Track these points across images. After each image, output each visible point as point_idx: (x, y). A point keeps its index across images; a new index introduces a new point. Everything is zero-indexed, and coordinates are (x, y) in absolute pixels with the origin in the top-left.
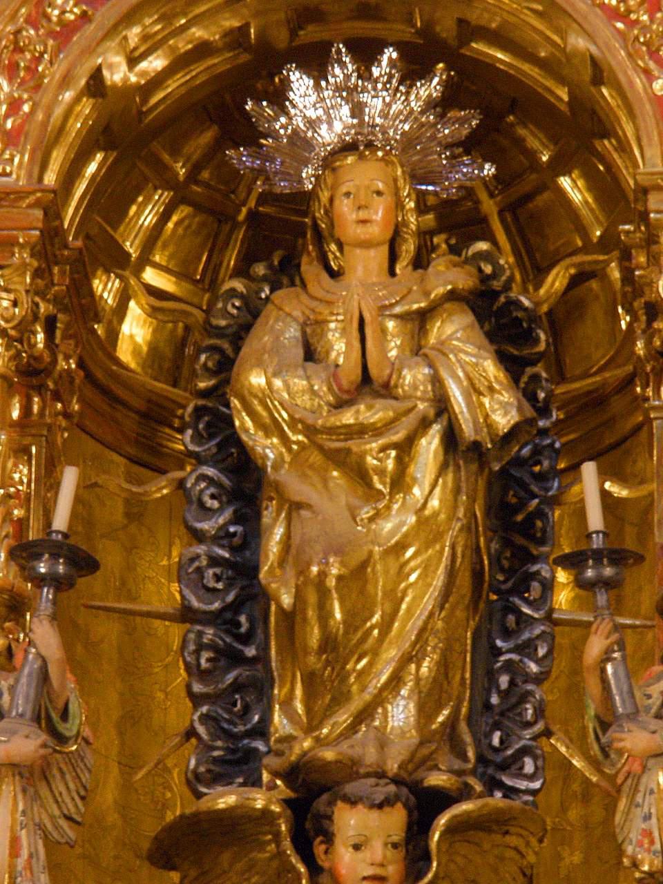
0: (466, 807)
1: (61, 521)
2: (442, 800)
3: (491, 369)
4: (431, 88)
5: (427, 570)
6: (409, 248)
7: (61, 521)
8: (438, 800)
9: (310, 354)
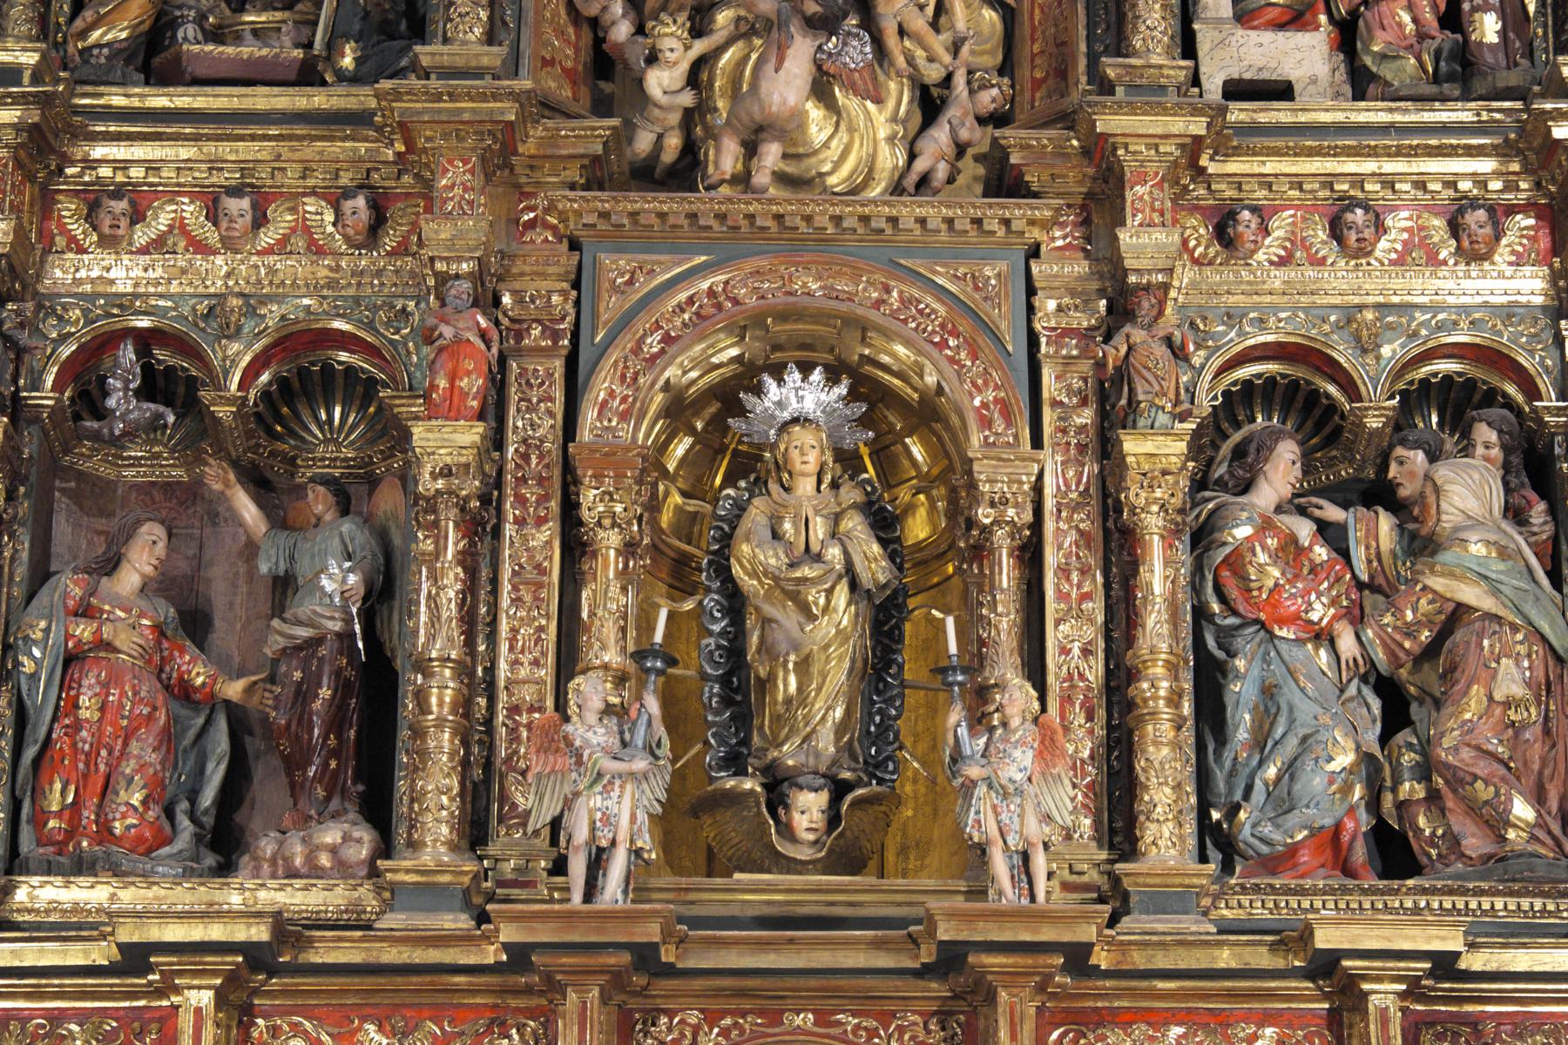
0: (860, 792)
1: (658, 637)
2: (848, 786)
3: (876, 548)
4: (842, 389)
5: (841, 658)
6: (828, 478)
7: (658, 637)
8: (848, 786)
9: (776, 535)
